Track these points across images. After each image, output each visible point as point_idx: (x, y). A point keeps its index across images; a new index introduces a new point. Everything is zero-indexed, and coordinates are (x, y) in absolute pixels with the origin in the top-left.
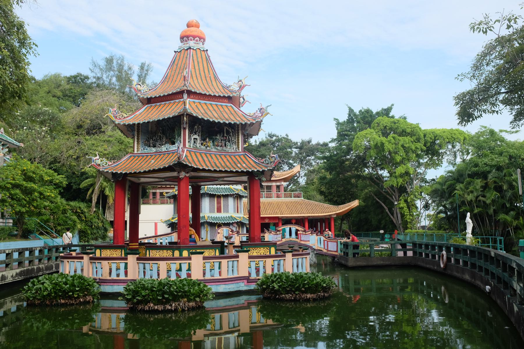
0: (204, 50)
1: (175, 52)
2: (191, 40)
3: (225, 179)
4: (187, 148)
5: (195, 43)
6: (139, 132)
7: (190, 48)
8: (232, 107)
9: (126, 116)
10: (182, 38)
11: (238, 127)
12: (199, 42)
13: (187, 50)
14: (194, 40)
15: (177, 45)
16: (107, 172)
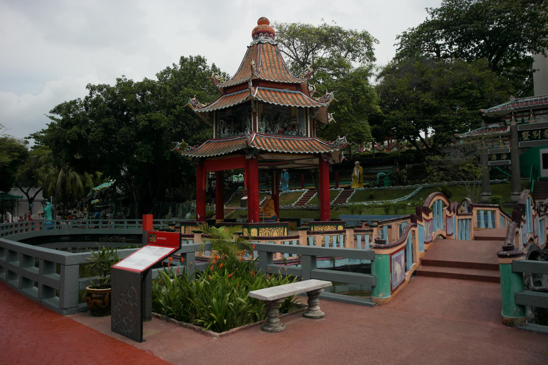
0: (273, 45)
1: (248, 47)
2: (261, 36)
3: (297, 162)
4: (256, 133)
5: (265, 38)
6: (217, 120)
7: (260, 43)
8: (300, 94)
9: (204, 106)
10: (253, 35)
11: (306, 111)
12: (269, 38)
13: (258, 44)
14: (264, 35)
15: (249, 40)
16: (188, 156)
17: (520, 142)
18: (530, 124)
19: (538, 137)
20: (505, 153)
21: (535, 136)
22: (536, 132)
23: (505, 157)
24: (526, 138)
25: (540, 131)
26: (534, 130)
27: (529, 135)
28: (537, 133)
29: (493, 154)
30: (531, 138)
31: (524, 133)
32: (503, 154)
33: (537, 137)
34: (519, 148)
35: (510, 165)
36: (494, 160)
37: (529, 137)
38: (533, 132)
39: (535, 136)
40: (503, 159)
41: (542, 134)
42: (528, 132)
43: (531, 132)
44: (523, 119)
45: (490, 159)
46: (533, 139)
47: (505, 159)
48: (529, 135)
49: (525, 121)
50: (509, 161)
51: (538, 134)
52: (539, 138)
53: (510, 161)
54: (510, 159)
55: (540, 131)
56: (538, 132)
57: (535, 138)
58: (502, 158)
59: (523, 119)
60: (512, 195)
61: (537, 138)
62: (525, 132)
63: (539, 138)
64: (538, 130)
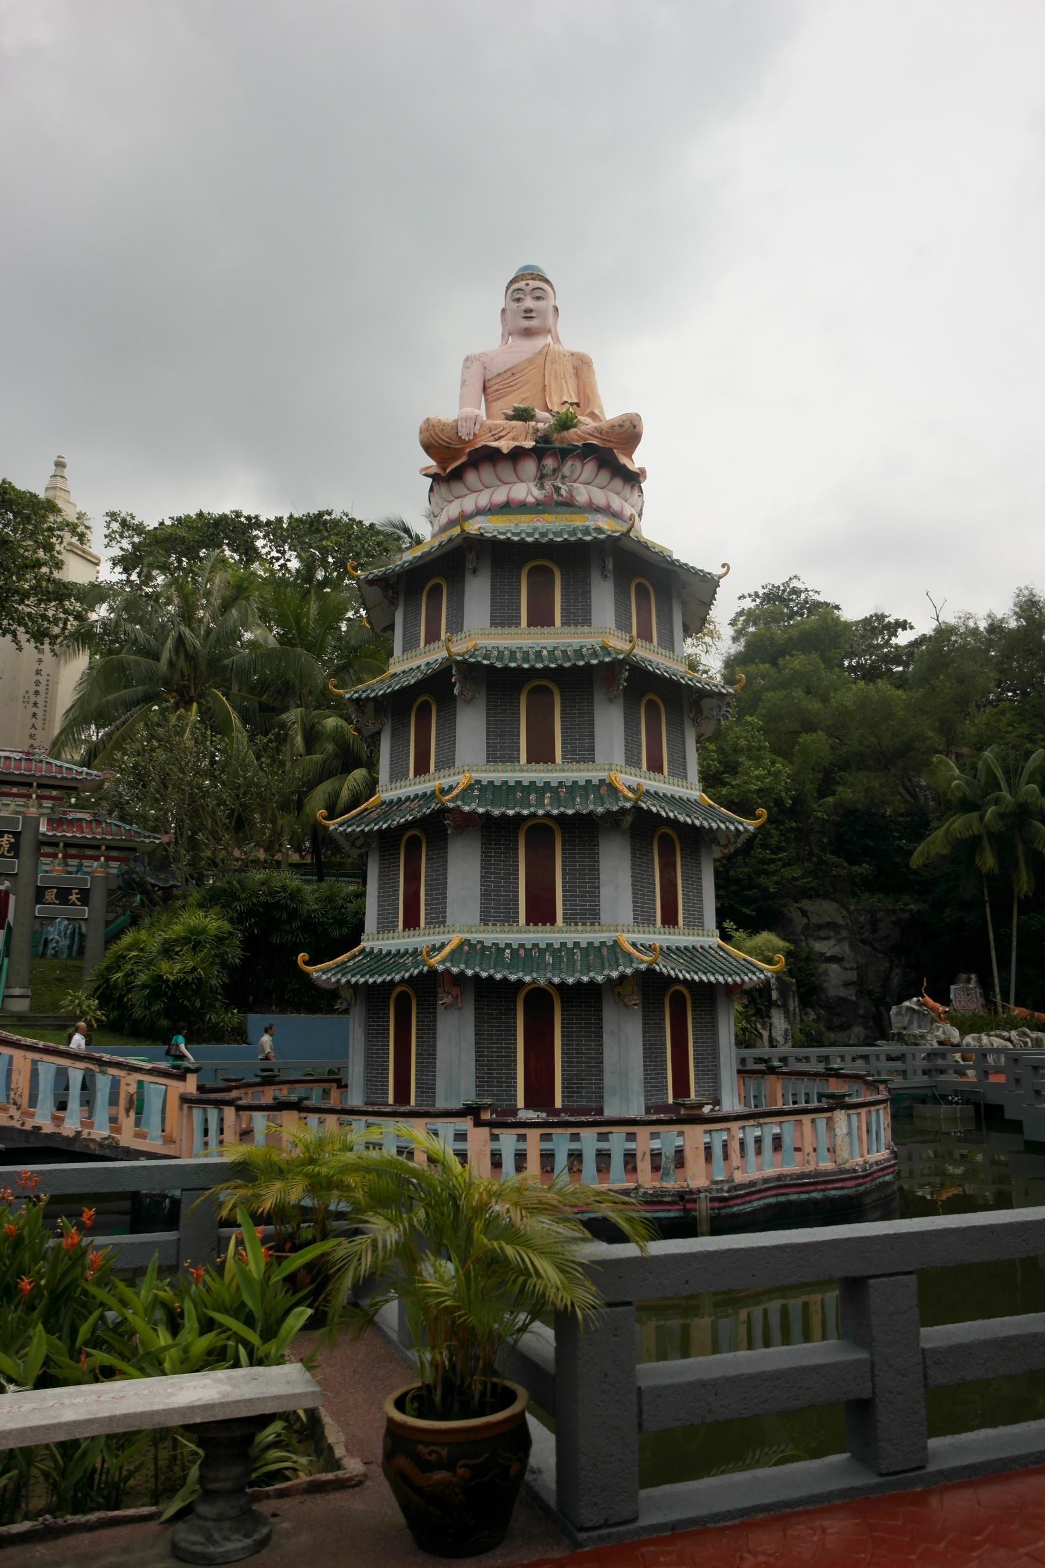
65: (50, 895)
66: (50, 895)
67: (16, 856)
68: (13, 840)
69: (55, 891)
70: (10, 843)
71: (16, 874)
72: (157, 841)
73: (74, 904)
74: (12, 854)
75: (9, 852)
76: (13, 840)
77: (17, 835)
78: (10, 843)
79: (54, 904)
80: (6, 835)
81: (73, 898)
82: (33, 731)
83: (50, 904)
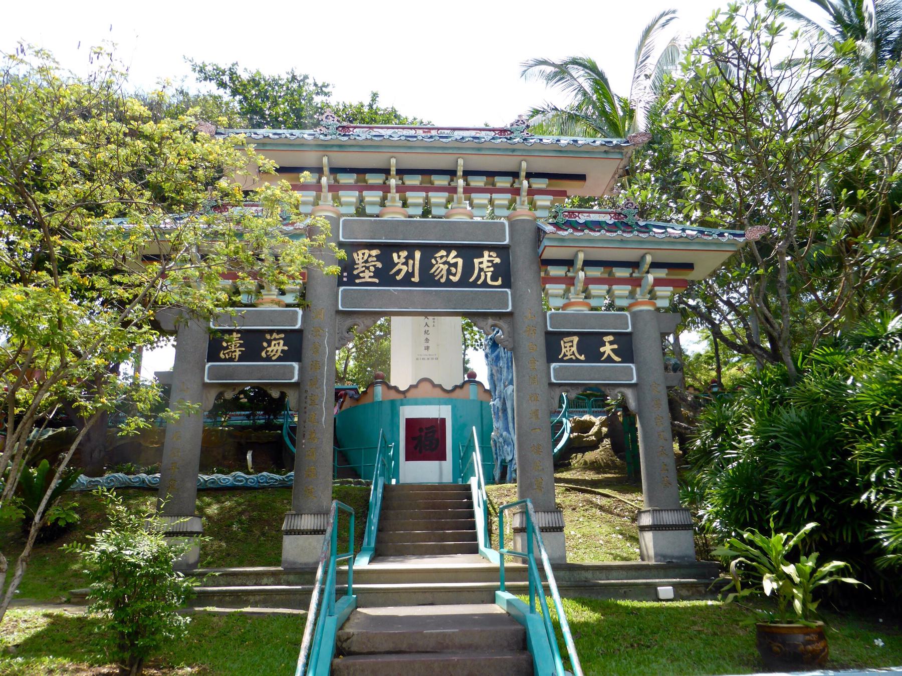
17: (341, 288)
18: (385, 218)
19: (412, 274)
20: (279, 332)
21: (400, 271)
22: (404, 254)
23: (277, 347)
24: (367, 276)
25: (418, 255)
26: (398, 247)
27: (379, 265)
28: (407, 258)
29: (230, 332)
30: (385, 276)
31: (360, 252)
32: (271, 332)
33: (410, 275)
34: (338, 312)
35: (297, 385)
36: (231, 360)
37: (377, 273)
38: (395, 255)
39: (400, 271)
40: (268, 359)
41: (426, 265)
42: (374, 252)
43: (387, 249)
44: (361, 200)
45: (213, 356)
46: (392, 281)
47: (279, 360)
48: (379, 265)
49: (369, 210)
50: (293, 367)
51: (411, 262)
52: (416, 279)
53: (296, 365)
54: (298, 359)
55: (418, 255)
56: (411, 256)
57: (399, 278)
58: (263, 354)
59: (361, 200)
60: (290, 532)
61: (407, 281)
62: (367, 252)
63: (416, 279)
64: (410, 248)
65: (569, 347)
66: (569, 347)
67: (507, 284)
68: (498, 260)
69: (576, 339)
70: (494, 265)
71: (510, 314)
72: (741, 240)
73: (609, 360)
74: (499, 282)
75: (494, 278)
76: (498, 260)
77: (502, 250)
78: (494, 265)
79: (578, 361)
80: (486, 253)
81: (607, 349)
82: (427, 328)
83: (571, 361)
